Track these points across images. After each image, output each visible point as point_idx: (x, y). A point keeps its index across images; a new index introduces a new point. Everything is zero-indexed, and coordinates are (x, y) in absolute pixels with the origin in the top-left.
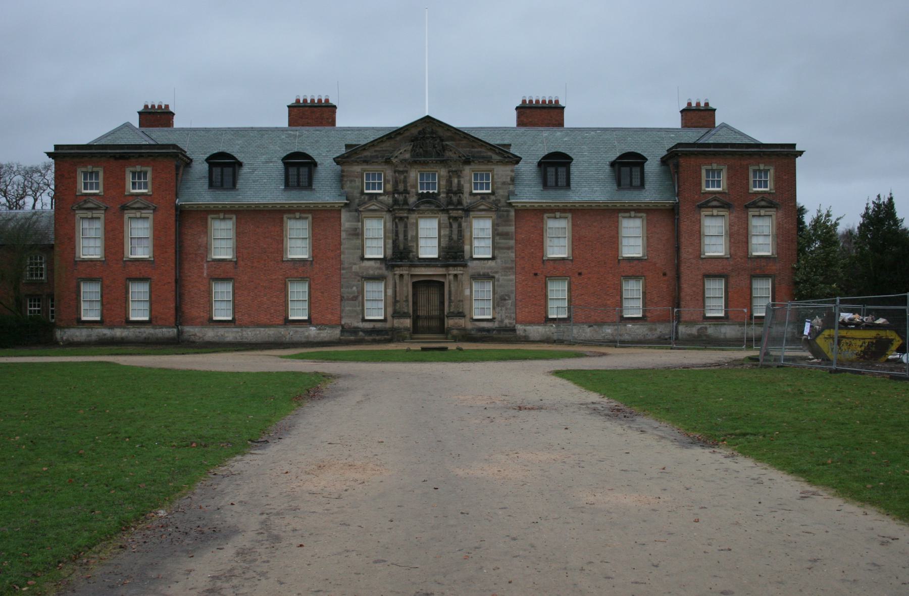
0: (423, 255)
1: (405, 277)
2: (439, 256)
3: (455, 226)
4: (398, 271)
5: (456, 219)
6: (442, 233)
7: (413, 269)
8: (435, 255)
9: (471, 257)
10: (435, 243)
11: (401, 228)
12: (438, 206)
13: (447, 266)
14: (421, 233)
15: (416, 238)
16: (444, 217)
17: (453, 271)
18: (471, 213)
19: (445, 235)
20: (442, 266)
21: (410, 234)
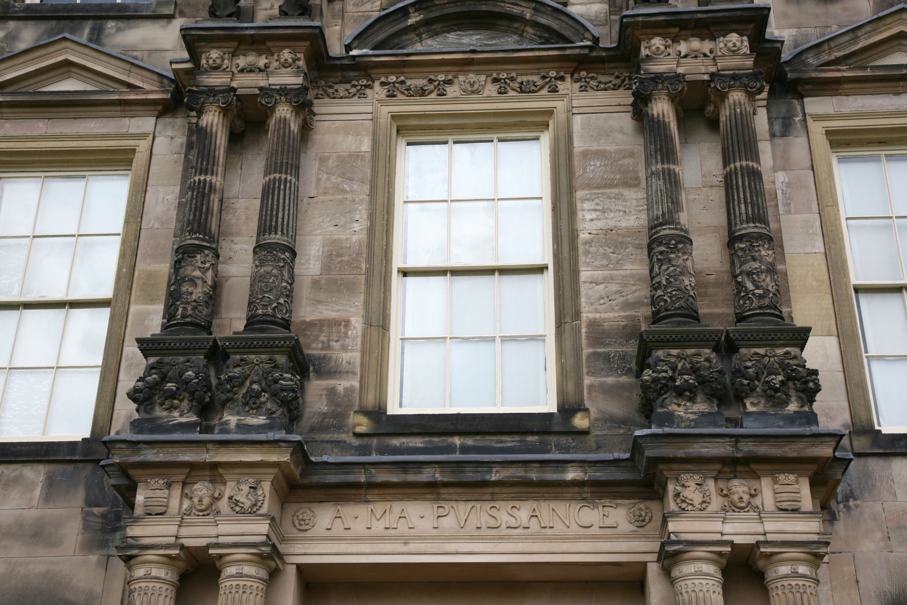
0: (421, 384)
1: (239, 584)
2: (568, 409)
3: (700, 165)
4: (166, 520)
5: (698, 105)
6: (590, 220)
7: (324, 517)
8: (528, 386)
9: (864, 428)
10: (532, 305)
11: (243, 189)
12: (550, 35)
13: (641, 481)
14: (418, 237)
15: (373, 268)
16: (597, 117)
17: (709, 516)
18: (815, 105)
19: (612, 239)
20: (597, 490)
21: (324, 231)
